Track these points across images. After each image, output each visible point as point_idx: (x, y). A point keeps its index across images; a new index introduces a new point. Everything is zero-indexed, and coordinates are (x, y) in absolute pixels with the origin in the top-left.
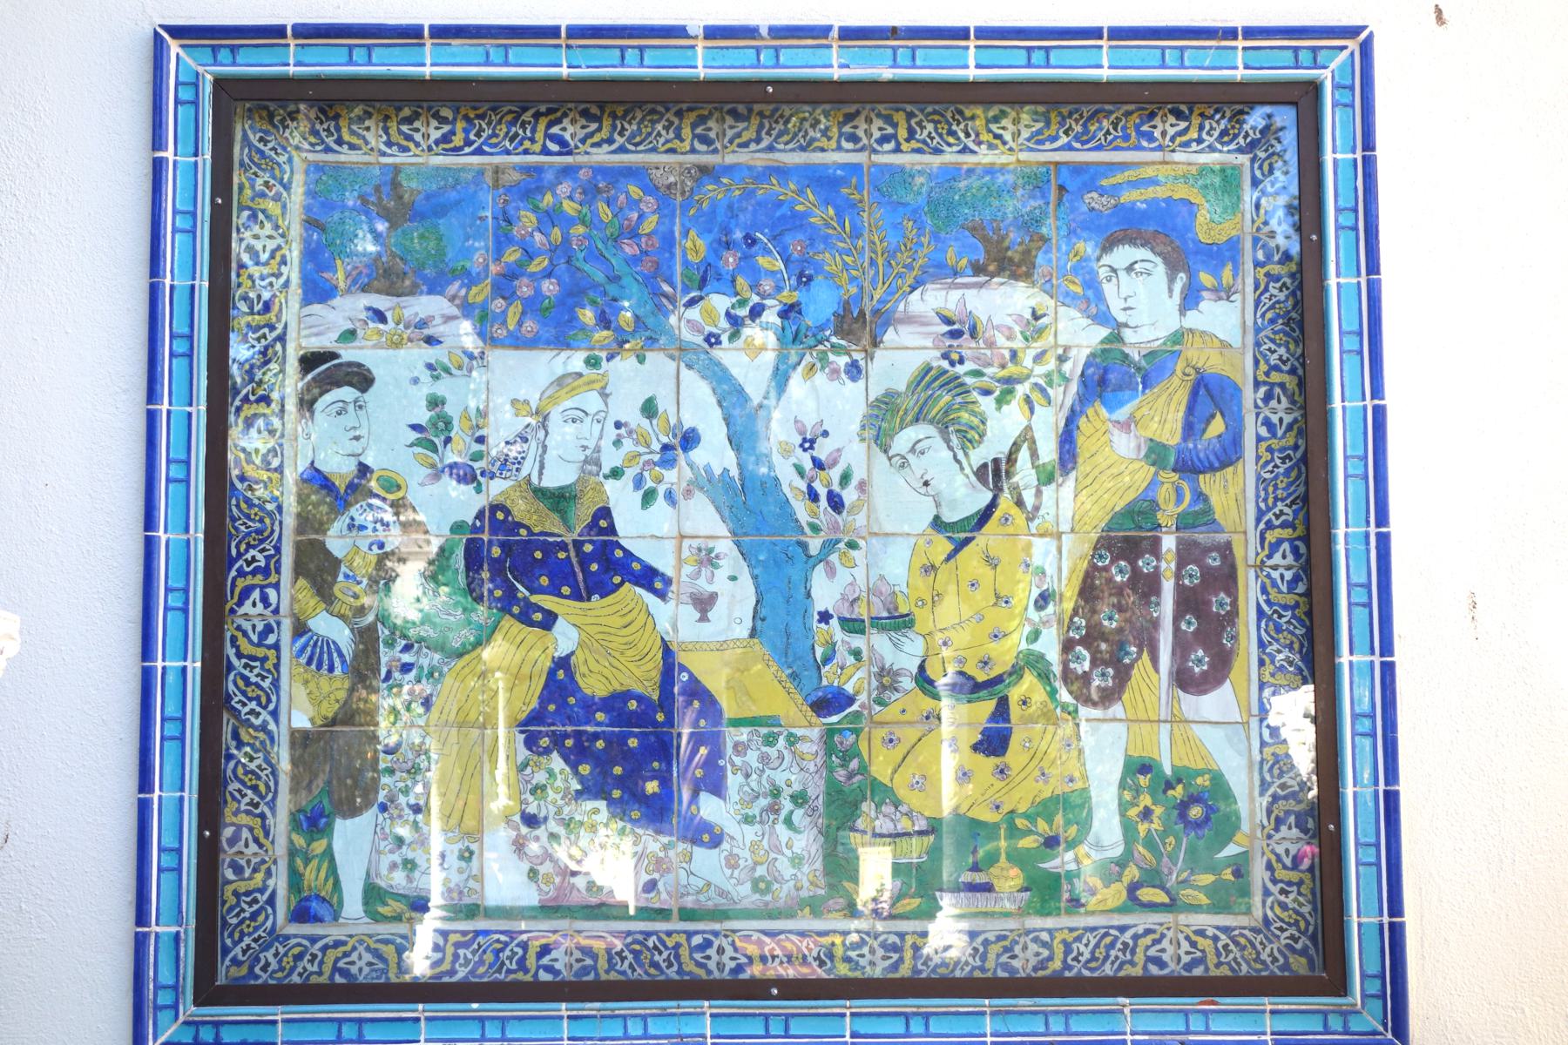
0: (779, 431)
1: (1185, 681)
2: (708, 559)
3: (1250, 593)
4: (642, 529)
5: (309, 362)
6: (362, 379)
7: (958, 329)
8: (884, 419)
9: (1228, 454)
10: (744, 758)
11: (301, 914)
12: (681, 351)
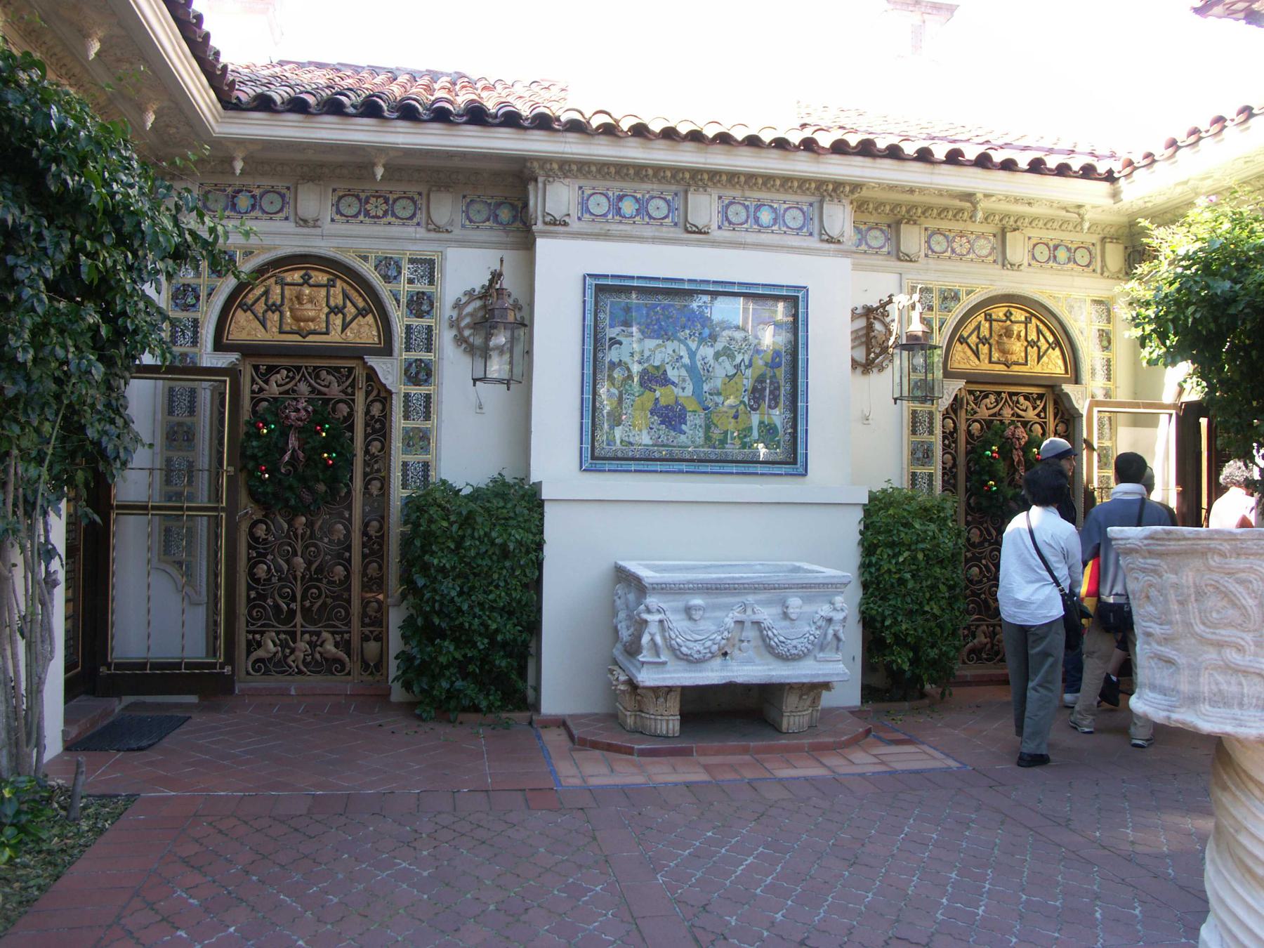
0: (698, 357)
1: (770, 407)
2: (684, 380)
3: (782, 390)
4: (672, 374)
5: (611, 339)
6: (620, 343)
7: (732, 339)
8: (717, 356)
9: (779, 365)
10: (689, 417)
11: (608, 444)
12: (680, 341)
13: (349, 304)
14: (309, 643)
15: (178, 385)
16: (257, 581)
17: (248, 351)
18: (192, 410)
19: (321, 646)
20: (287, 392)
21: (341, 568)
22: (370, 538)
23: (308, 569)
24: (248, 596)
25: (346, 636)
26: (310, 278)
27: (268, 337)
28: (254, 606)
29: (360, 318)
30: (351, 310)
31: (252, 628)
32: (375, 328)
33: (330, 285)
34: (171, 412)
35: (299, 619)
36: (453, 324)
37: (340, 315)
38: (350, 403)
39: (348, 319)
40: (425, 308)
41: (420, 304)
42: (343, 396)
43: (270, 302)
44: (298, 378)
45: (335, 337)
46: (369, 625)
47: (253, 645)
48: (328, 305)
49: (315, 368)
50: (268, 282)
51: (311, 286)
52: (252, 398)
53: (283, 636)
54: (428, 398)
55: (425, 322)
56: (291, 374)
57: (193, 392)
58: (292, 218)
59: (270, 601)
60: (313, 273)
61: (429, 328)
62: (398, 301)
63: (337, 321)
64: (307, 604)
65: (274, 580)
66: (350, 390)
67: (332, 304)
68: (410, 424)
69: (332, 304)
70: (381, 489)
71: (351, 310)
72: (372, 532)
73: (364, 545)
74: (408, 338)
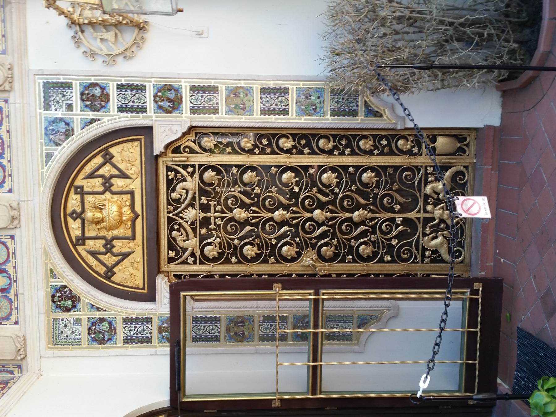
13: (100, 172)
14: (435, 205)
15: (190, 333)
16: (375, 254)
17: (153, 268)
18: (215, 320)
19: (438, 194)
20: (194, 230)
21: (365, 175)
22: (335, 147)
23: (364, 207)
24: (388, 262)
25: (430, 170)
26: (74, 212)
27: (139, 251)
28: (399, 256)
29: (114, 160)
30: (107, 170)
31: (419, 258)
32: (125, 145)
33: (81, 191)
34: (216, 339)
35: (412, 215)
36: (111, 59)
37: (113, 181)
38: (204, 168)
39: (117, 173)
40: (97, 92)
41: (95, 97)
42: (196, 176)
43: (103, 250)
44: (180, 220)
45: (136, 185)
46: (420, 148)
47: (436, 257)
48: (103, 193)
49: (169, 203)
50: (84, 254)
51: (83, 211)
52: (201, 262)
53: (428, 230)
54: (194, 89)
55: (113, 92)
56: (176, 227)
57: (196, 319)
58: (12, 233)
59: (394, 242)
60: (69, 210)
61: (120, 87)
62: (92, 121)
63: (119, 184)
64: (398, 207)
65: (373, 238)
66: (190, 170)
67: (101, 189)
68: (222, 107)
69: (101, 189)
70: (288, 138)
71: (107, 170)
72: (330, 145)
73: (342, 153)
74: (132, 110)
